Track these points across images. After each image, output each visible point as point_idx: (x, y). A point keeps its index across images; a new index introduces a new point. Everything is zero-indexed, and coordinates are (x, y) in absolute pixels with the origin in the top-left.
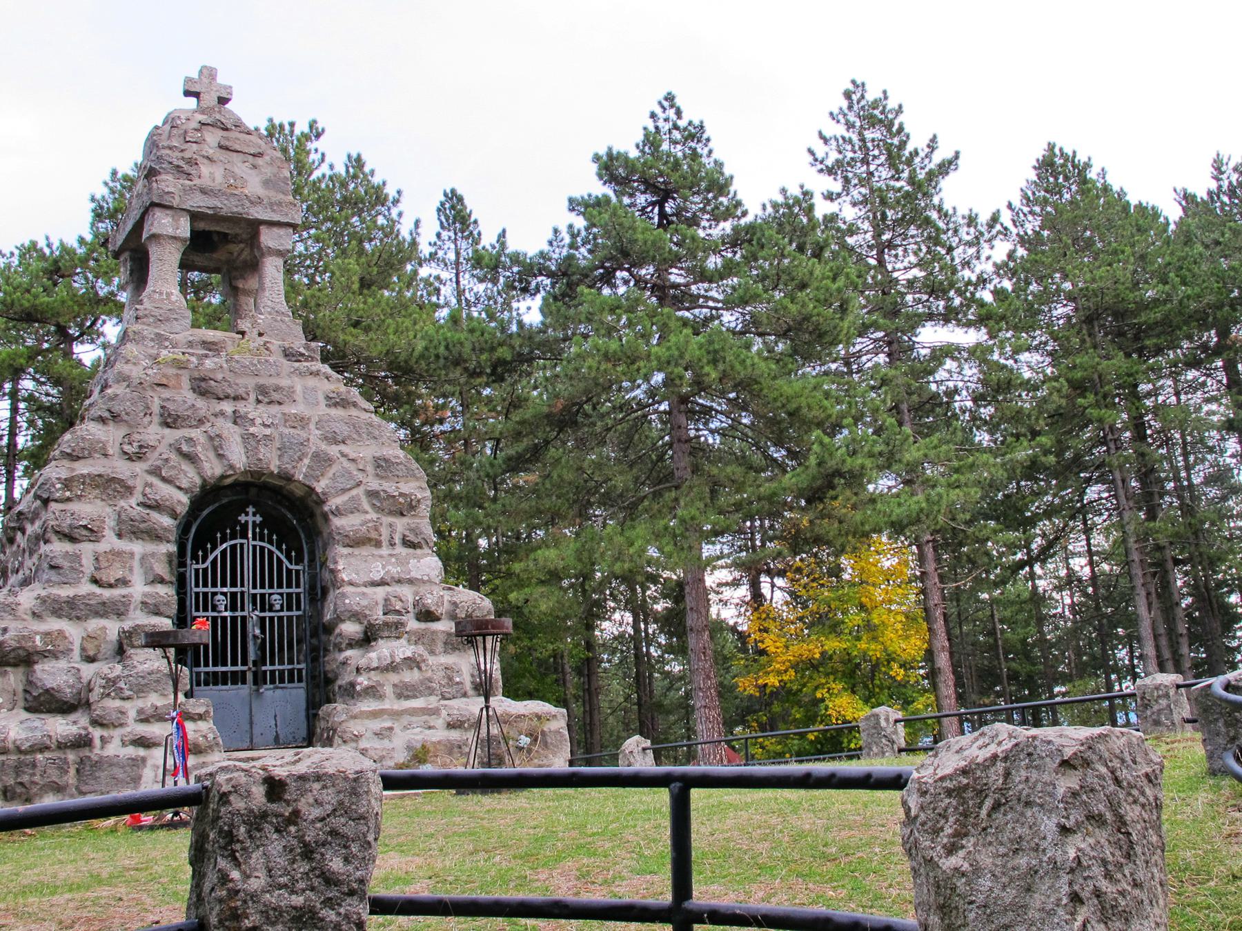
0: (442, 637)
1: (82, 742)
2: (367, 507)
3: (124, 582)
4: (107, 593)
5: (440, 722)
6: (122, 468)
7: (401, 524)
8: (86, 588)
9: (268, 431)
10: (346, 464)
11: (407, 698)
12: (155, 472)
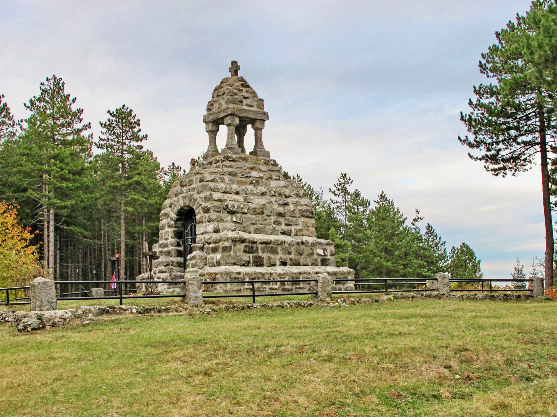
0: (210, 249)
2: (201, 212)
3: (167, 239)
4: (166, 242)
5: (198, 275)
7: (207, 215)
8: (164, 241)
9: (185, 194)
10: (199, 199)
11: (194, 267)
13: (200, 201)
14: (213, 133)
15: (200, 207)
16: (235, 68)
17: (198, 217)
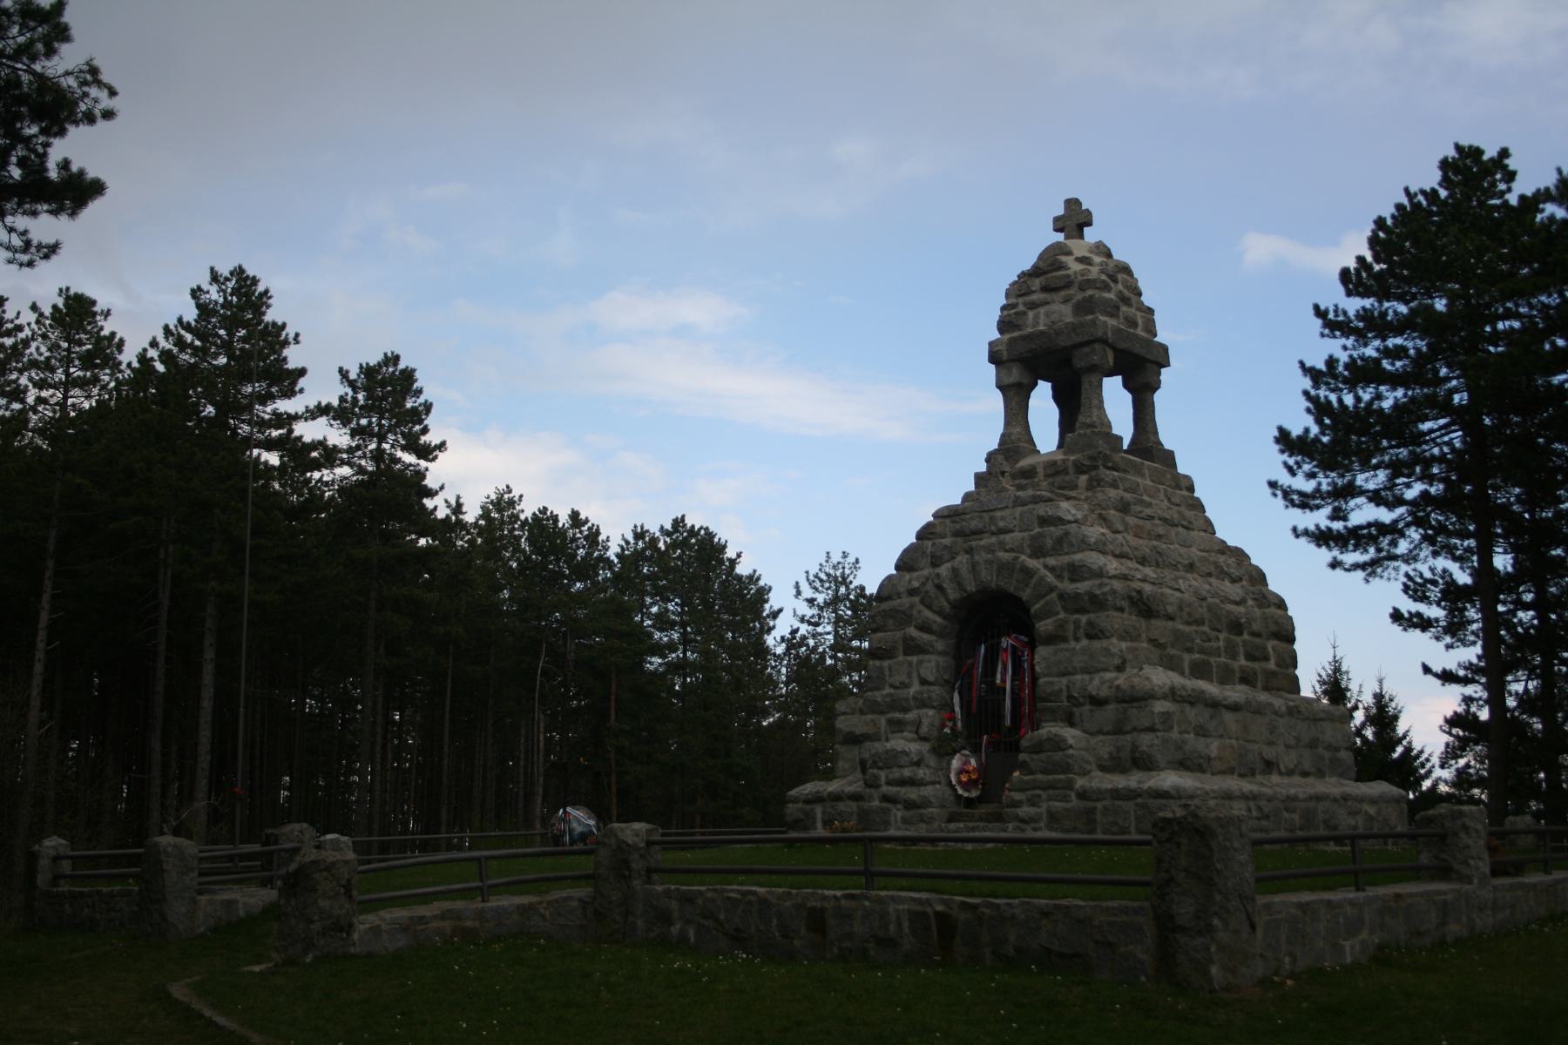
1: (856, 797)
2: (1059, 608)
6: (905, 601)
10: (1043, 571)
12: (922, 602)
13: (1050, 578)
14: (1016, 397)
15: (1054, 595)
16: (1074, 219)
17: (1044, 626)
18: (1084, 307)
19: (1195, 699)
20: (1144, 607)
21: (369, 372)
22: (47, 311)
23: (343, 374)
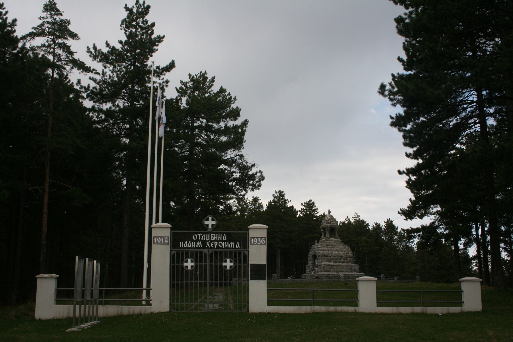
18: (327, 223)
19: (329, 265)
20: (326, 256)
21: (307, 203)
22: (251, 200)
23: (302, 204)
